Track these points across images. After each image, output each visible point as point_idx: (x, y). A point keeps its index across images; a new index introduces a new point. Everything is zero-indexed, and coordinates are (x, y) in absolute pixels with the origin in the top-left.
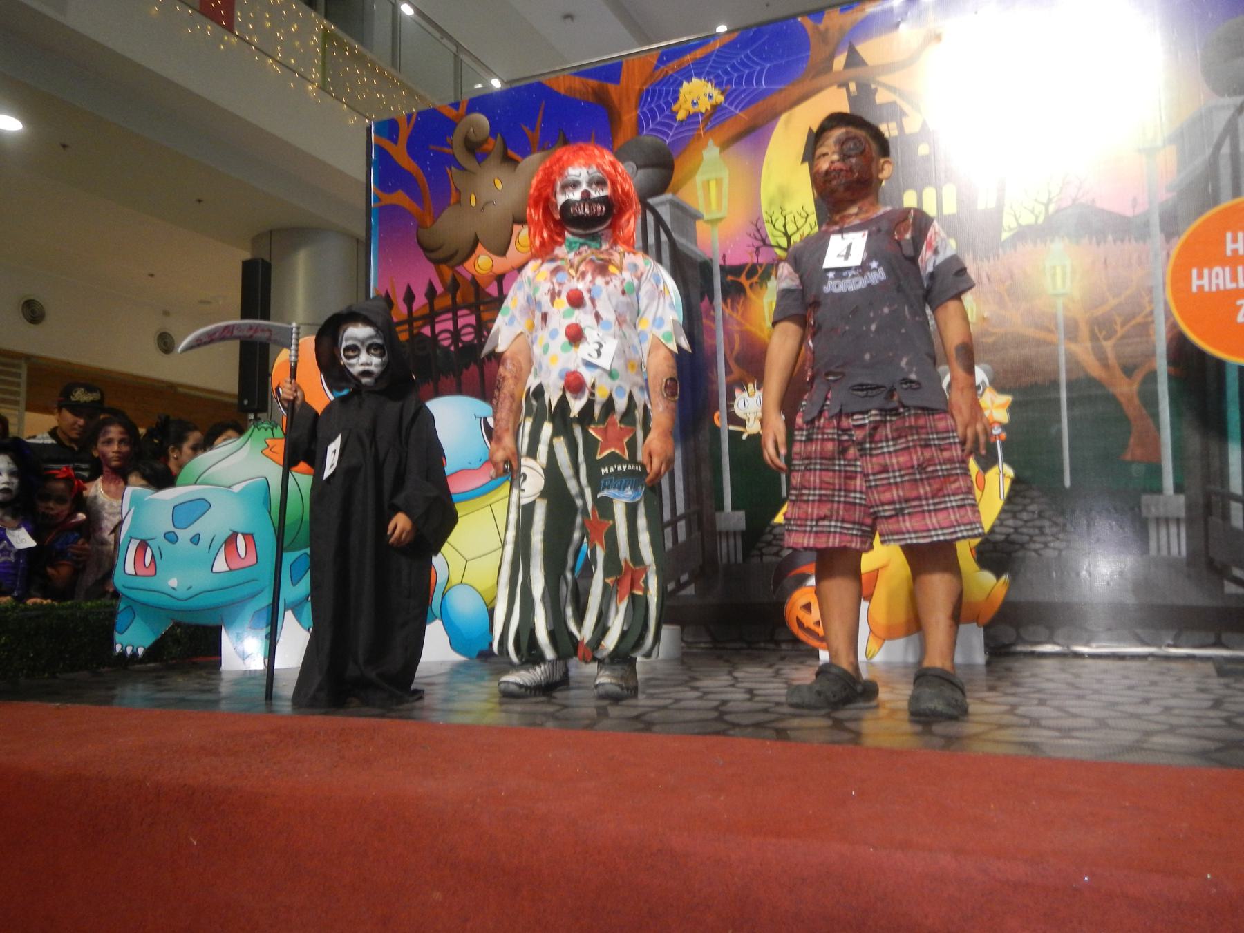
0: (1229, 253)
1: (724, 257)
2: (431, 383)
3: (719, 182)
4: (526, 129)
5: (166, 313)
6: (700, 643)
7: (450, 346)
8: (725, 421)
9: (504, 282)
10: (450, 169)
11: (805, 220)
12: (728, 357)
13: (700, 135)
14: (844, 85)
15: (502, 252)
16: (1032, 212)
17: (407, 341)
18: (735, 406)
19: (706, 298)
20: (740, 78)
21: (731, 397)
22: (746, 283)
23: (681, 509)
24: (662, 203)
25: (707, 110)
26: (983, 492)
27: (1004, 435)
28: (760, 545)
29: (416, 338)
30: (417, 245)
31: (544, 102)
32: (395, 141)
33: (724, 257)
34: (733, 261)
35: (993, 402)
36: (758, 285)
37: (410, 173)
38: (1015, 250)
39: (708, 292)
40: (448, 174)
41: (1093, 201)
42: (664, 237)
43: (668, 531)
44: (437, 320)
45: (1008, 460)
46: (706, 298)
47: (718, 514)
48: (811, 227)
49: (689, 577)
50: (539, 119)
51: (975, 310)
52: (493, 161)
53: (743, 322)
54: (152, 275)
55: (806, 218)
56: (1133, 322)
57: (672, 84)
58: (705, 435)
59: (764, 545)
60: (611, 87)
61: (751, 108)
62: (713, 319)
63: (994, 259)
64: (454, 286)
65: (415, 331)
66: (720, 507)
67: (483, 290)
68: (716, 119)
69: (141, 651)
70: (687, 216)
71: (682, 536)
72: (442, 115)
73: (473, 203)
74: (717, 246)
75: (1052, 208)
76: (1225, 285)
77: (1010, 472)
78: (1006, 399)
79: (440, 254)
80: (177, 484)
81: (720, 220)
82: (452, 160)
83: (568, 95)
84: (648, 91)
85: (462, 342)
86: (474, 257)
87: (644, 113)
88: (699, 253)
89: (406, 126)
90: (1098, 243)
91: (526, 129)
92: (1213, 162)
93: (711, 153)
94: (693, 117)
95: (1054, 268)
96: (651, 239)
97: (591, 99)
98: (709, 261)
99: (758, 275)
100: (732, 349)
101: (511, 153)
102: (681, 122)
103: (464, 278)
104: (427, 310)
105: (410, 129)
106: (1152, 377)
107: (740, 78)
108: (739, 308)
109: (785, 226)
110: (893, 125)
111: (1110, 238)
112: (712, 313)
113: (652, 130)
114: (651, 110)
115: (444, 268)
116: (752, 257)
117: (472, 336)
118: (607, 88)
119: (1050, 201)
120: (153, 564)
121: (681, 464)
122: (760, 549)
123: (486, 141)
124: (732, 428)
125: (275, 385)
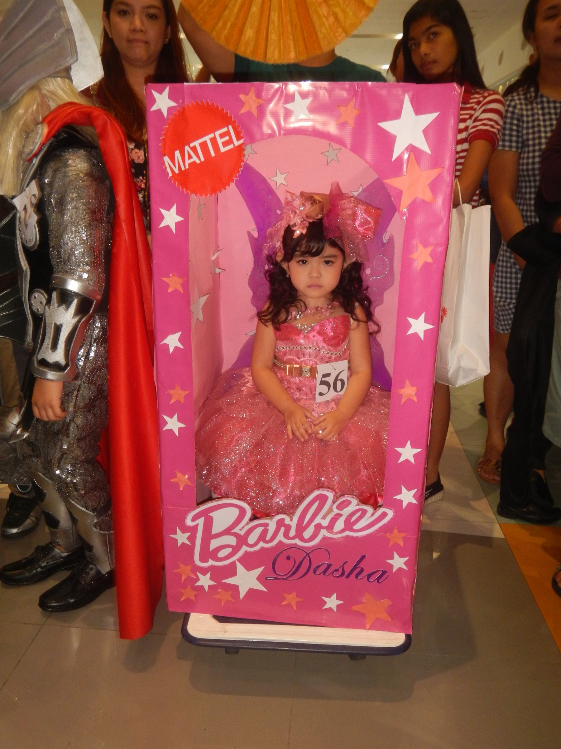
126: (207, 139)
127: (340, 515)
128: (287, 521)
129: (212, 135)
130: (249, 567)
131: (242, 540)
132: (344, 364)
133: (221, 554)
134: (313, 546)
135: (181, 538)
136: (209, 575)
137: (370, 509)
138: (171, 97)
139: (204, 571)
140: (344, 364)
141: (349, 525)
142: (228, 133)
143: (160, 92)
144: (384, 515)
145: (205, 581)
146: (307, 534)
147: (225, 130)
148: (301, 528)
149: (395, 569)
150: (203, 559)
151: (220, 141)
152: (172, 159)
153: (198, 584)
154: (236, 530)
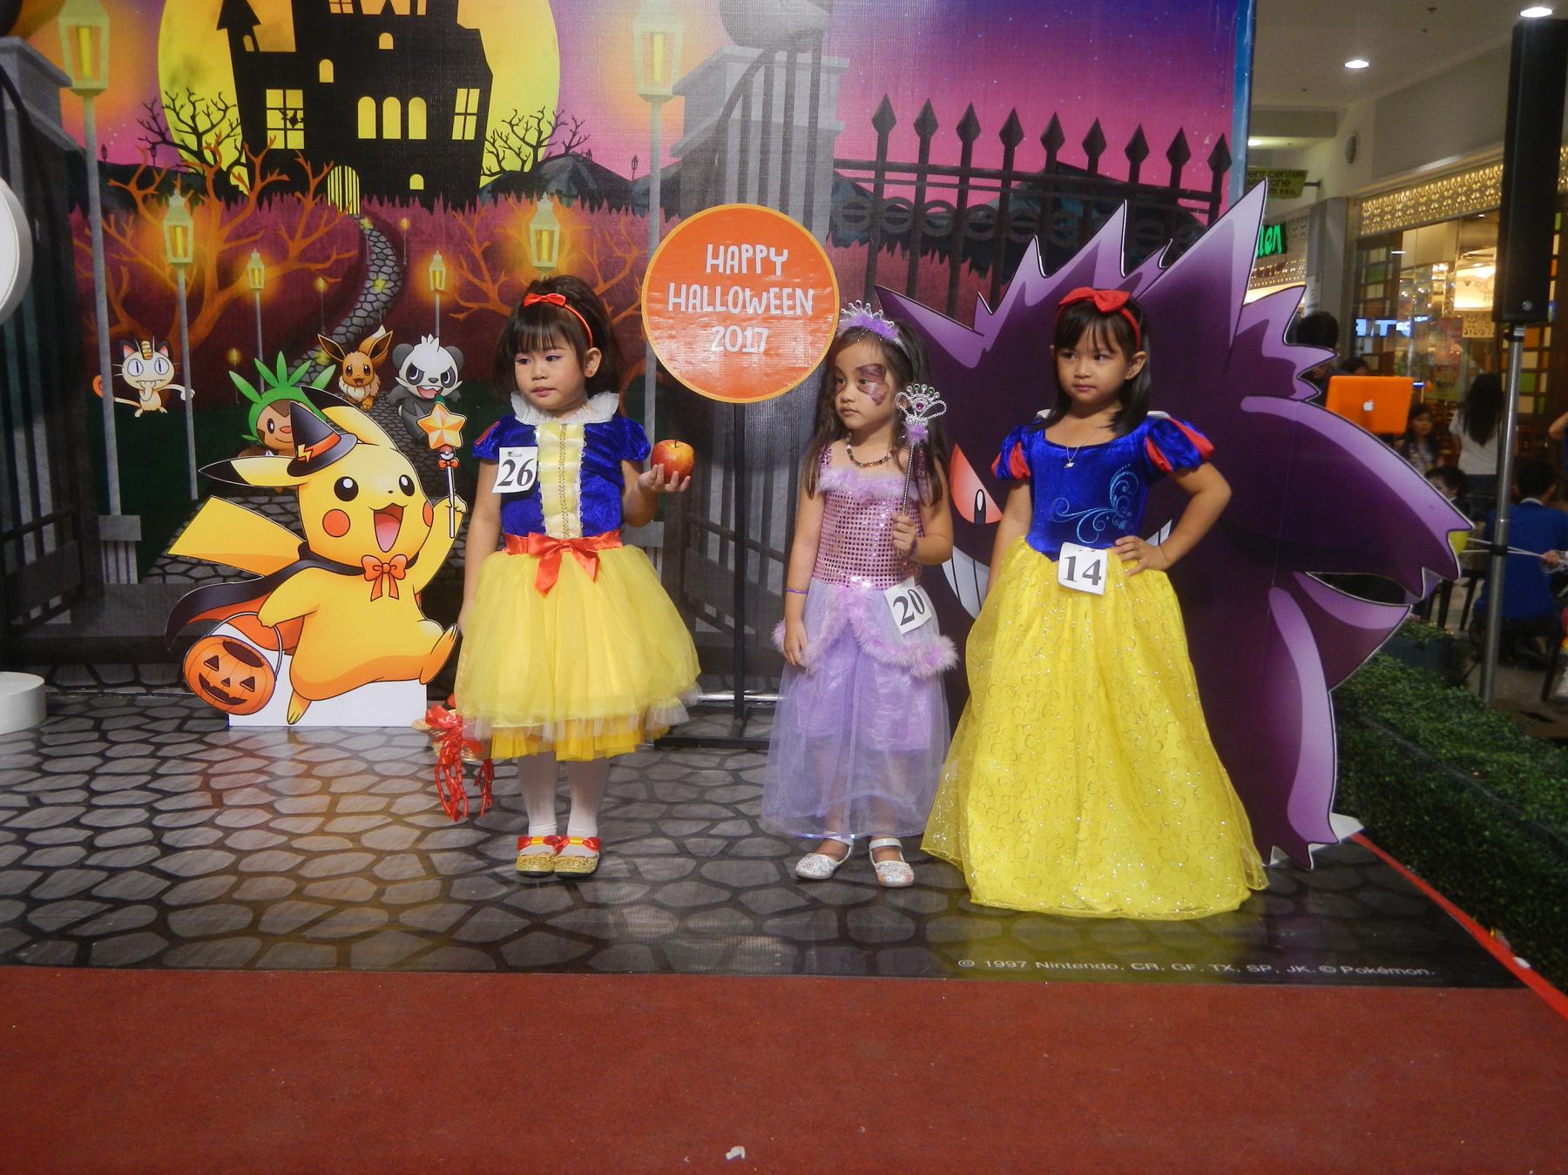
0: (709, 270)
1: (104, 149)
3: (95, 32)
8: (110, 389)
11: (222, 113)
12: (112, 298)
16: (518, 155)
18: (124, 370)
19: (77, 208)
21: (118, 358)
22: (138, 195)
23: (47, 508)
27: (456, 462)
28: (161, 561)
33: (104, 149)
34: (118, 157)
35: (443, 422)
36: (155, 200)
38: (496, 204)
41: (589, 153)
43: (29, 537)
45: (459, 492)
46: (77, 208)
47: (101, 517)
48: (231, 125)
49: (63, 600)
51: (444, 274)
53: (133, 250)
55: (225, 111)
56: (624, 314)
59: (168, 561)
63: (470, 209)
66: (106, 510)
70: (49, 79)
71: (50, 546)
74: (93, 130)
75: (541, 153)
76: (702, 307)
77: (462, 506)
78: (459, 420)
81: (97, 92)
88: (66, 138)
92: (721, 129)
95: (539, 232)
98: (81, 152)
99: (155, 185)
100: (118, 289)
106: (640, 380)
109: (193, 118)
111: (605, 203)
112: (87, 230)
116: (146, 160)
119: (539, 144)
121: (45, 443)
122: (162, 567)
124: (118, 400)
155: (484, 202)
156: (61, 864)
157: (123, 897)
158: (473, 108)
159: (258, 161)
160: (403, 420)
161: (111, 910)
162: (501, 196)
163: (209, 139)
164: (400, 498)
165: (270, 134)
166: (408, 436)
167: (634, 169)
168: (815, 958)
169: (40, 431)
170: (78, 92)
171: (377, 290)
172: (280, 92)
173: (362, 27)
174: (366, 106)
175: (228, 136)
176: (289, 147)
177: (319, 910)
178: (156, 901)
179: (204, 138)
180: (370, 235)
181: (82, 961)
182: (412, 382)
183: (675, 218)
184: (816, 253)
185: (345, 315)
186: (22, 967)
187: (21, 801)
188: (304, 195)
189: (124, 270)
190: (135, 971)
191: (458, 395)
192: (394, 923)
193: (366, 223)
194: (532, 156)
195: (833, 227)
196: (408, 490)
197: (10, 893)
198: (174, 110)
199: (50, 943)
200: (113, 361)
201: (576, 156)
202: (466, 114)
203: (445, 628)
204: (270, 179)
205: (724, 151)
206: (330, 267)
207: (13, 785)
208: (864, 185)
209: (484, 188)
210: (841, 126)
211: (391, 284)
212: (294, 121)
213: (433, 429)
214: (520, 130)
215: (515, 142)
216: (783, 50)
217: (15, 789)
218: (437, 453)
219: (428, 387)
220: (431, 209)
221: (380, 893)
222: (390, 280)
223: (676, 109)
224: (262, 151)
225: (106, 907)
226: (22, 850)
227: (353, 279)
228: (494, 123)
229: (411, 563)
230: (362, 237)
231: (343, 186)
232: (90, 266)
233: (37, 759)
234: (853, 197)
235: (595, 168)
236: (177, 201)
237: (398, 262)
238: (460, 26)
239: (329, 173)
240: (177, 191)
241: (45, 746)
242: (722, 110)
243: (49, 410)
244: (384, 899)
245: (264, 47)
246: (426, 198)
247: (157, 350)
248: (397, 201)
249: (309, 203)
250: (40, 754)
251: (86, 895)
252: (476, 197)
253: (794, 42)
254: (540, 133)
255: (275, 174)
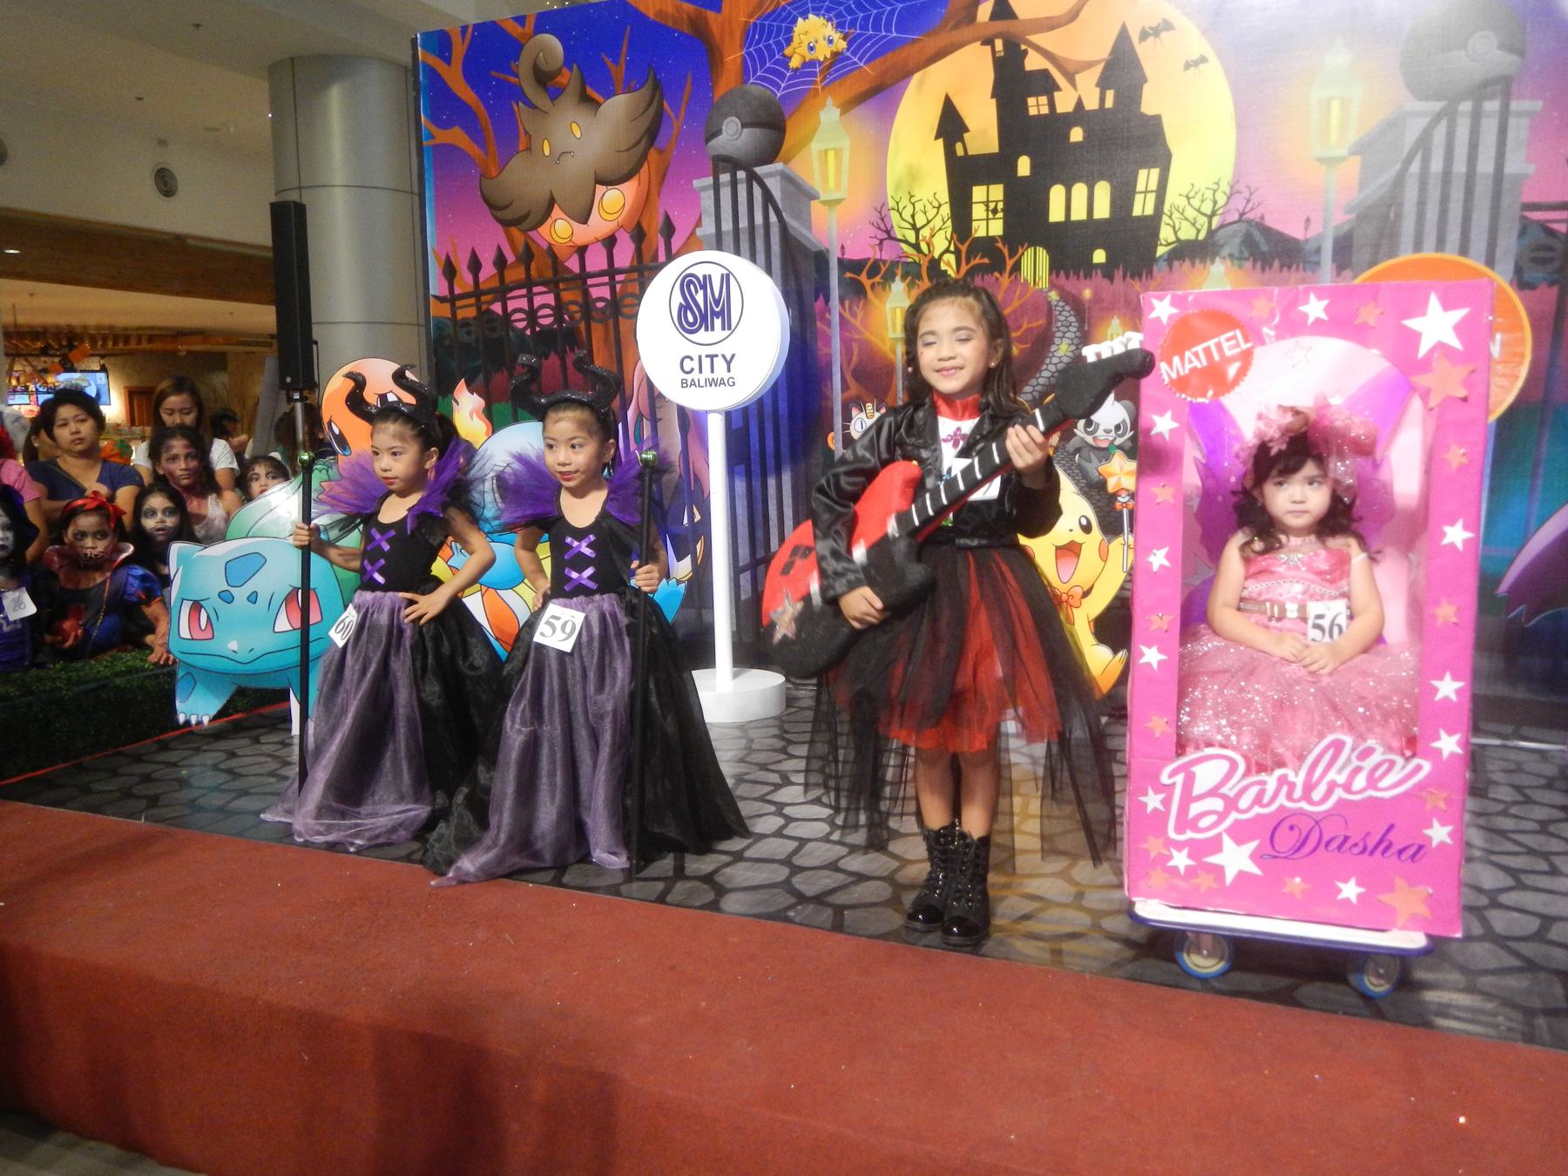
1: (843, 247)
2: (506, 373)
3: (838, 152)
4: (608, 61)
5: (163, 142)
6: (806, 685)
7: (525, 328)
9: (588, 255)
10: (518, 105)
11: (936, 210)
12: (845, 366)
13: (817, 89)
14: (989, 42)
15: (584, 219)
16: (1194, 225)
17: (475, 318)
18: (852, 428)
19: (821, 297)
20: (866, 19)
21: (847, 418)
22: (867, 283)
24: (771, 175)
25: (825, 57)
26: (1105, 562)
29: (484, 315)
30: (481, 200)
31: (629, 27)
32: (448, 61)
33: (843, 247)
35: (1121, 468)
37: (469, 107)
38: (1171, 266)
39: (823, 290)
40: (513, 112)
41: (1262, 218)
42: (773, 218)
44: (509, 296)
46: (821, 297)
50: (624, 50)
52: (568, 101)
53: (862, 329)
54: (141, 99)
55: (938, 208)
57: (782, 21)
58: (817, 458)
60: (711, 15)
61: (878, 61)
62: (828, 324)
64: (527, 256)
65: (484, 307)
67: (562, 263)
68: (836, 71)
69: (206, 720)
70: (801, 193)
72: (503, 29)
73: (547, 153)
74: (834, 233)
75: (1216, 222)
79: (507, 215)
80: (227, 538)
81: (838, 202)
82: (520, 95)
83: (658, 20)
84: (755, 24)
85: (540, 325)
86: (549, 221)
87: (749, 54)
88: (814, 240)
89: (460, 40)
90: (1263, 270)
91: (608, 61)
92: (1399, 182)
93: (829, 114)
94: (809, 64)
96: (759, 219)
97: (686, 31)
100: (850, 361)
101: (590, 91)
102: (797, 69)
103: (538, 244)
104: (495, 283)
105: (465, 47)
107: (866, 19)
108: (858, 311)
110: (1043, 100)
111: (1276, 264)
113: (760, 78)
114: (759, 51)
115: (514, 231)
116: (875, 252)
117: (551, 319)
118: (706, 17)
119: (1214, 213)
120: (209, 627)
123: (559, 72)
125: (326, 420)
126: (1211, 343)
127: (1358, 770)
128: (1292, 777)
129: (1216, 340)
130: (1239, 840)
131: (1231, 804)
132: (1340, 606)
133: (1204, 823)
134: (1326, 811)
135: (1153, 801)
136: (1185, 852)
137: (1400, 760)
138: (1173, 304)
139: (1179, 846)
140: (1340, 606)
141: (1372, 782)
142: (1235, 337)
143: (1161, 299)
144: (1418, 768)
145: (1181, 860)
146: (1317, 795)
147: (1230, 334)
148: (1309, 788)
149: (1435, 843)
150: (1180, 829)
151: (1225, 345)
152: (1170, 364)
153: (1171, 863)
154: (1225, 790)
155: (1160, 269)
156: (811, 837)
157: (864, 872)
158: (1153, 185)
159: (964, 248)
160: (1080, 467)
161: (854, 883)
162: (1176, 264)
163: (925, 233)
164: (1079, 536)
165: (975, 224)
166: (1084, 481)
167: (1306, 228)
168: (1545, 1027)
169: (787, 478)
170: (825, 203)
171: (1061, 353)
172: (985, 187)
173: (1057, 123)
174: (1057, 193)
175: (940, 229)
176: (990, 234)
177: (1029, 907)
178: (890, 879)
179: (921, 232)
180: (1056, 306)
181: (838, 926)
182: (1089, 433)
183: (1347, 273)
184: (1509, 299)
185: (1032, 377)
186: (791, 926)
187: (775, 778)
188: (1001, 274)
189: (855, 345)
190: (881, 942)
191: (1130, 444)
192: (1097, 927)
193: (1054, 296)
194: (1206, 226)
195: (1518, 271)
196: (1087, 529)
197: (777, 858)
198: (898, 211)
199: (811, 906)
200: (843, 421)
201: (1249, 222)
202: (1146, 192)
203: (1115, 652)
204: (973, 262)
205: (1400, 205)
206: (1022, 335)
207: (771, 763)
208: (1555, 226)
209: (1160, 257)
210: (1531, 169)
211: (1074, 347)
212: (995, 211)
213: (1112, 475)
214: (1196, 202)
215: (1190, 213)
216: (1463, 100)
217: (770, 767)
218: (1114, 496)
219: (1102, 438)
220: (1111, 278)
221: (1080, 896)
222: (1073, 344)
223: (1353, 166)
224: (965, 242)
225: (850, 879)
226: (780, 821)
227: (1042, 342)
228: (1172, 197)
229: (1086, 594)
230: (1050, 310)
231: (1035, 264)
232: (828, 343)
233: (780, 744)
234: (1542, 237)
235: (1267, 231)
236: (898, 286)
237: (1080, 329)
238: (1144, 115)
239: (1023, 254)
240: (898, 278)
241: (787, 732)
242: (1398, 166)
243: (794, 461)
244: (1085, 903)
245: (973, 150)
246: (1108, 270)
247: (878, 411)
248: (1082, 274)
249: (1005, 280)
250: (783, 739)
251: (834, 866)
252: (1152, 267)
253: (1480, 91)
254: (1215, 203)
255: (979, 256)
